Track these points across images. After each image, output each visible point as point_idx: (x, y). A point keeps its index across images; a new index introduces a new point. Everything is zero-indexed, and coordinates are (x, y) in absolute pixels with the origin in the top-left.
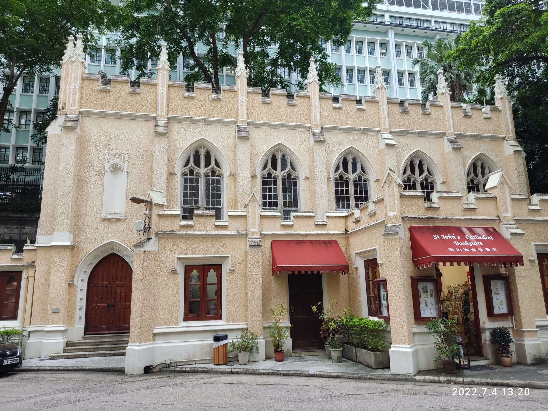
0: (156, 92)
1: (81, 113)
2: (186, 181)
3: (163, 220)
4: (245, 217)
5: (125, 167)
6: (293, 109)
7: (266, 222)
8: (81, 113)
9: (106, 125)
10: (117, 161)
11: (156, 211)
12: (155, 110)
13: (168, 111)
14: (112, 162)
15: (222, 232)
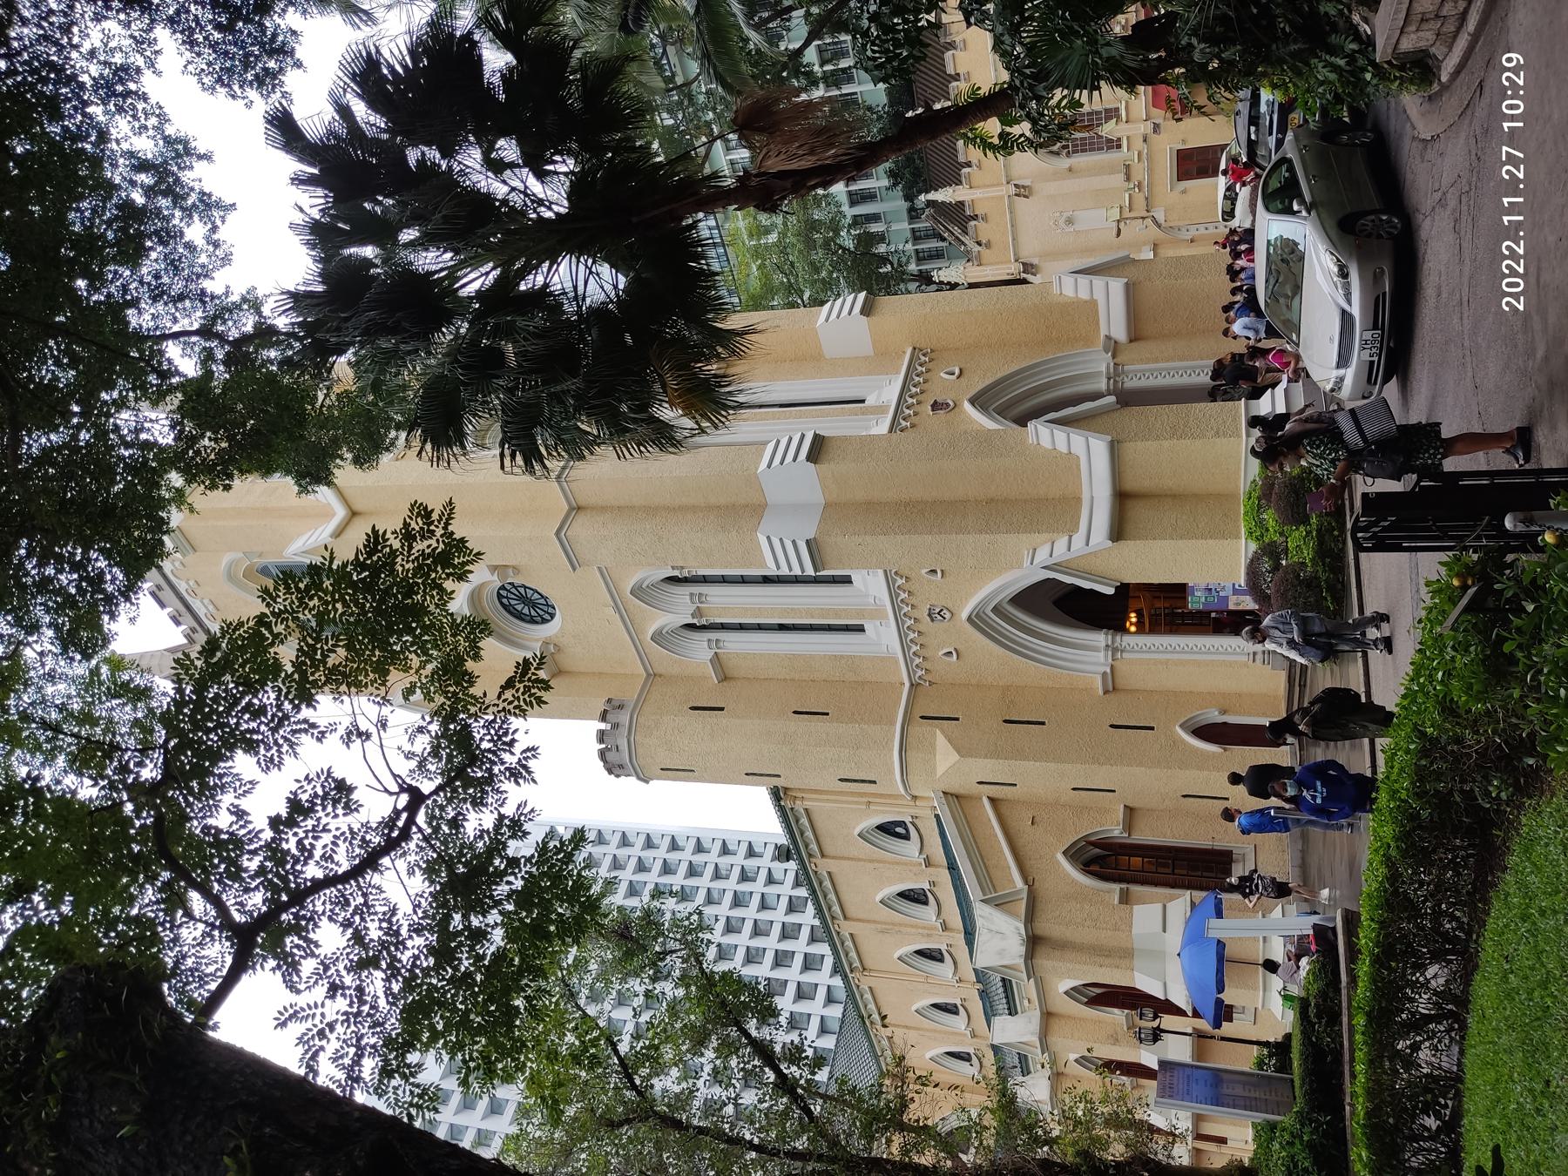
0: (981, 199)
1: (1016, 261)
2: (1077, 152)
3: (1135, 206)
4: (1128, 138)
5: (1066, 215)
6: (968, 42)
7: (1133, 115)
8: (1016, 261)
9: (1023, 239)
10: (1061, 222)
11: (1127, 214)
12: (1002, 197)
13: (998, 185)
14: (1063, 226)
15: (1145, 155)
